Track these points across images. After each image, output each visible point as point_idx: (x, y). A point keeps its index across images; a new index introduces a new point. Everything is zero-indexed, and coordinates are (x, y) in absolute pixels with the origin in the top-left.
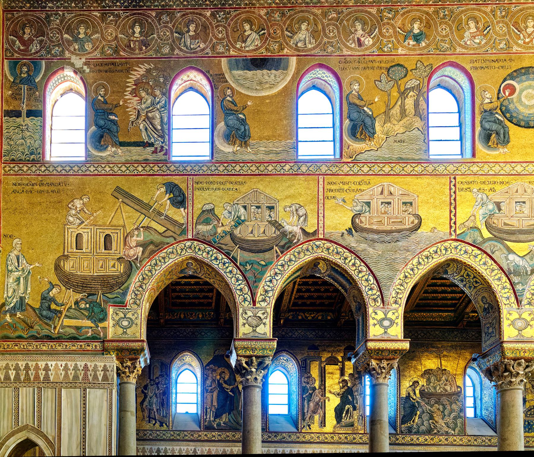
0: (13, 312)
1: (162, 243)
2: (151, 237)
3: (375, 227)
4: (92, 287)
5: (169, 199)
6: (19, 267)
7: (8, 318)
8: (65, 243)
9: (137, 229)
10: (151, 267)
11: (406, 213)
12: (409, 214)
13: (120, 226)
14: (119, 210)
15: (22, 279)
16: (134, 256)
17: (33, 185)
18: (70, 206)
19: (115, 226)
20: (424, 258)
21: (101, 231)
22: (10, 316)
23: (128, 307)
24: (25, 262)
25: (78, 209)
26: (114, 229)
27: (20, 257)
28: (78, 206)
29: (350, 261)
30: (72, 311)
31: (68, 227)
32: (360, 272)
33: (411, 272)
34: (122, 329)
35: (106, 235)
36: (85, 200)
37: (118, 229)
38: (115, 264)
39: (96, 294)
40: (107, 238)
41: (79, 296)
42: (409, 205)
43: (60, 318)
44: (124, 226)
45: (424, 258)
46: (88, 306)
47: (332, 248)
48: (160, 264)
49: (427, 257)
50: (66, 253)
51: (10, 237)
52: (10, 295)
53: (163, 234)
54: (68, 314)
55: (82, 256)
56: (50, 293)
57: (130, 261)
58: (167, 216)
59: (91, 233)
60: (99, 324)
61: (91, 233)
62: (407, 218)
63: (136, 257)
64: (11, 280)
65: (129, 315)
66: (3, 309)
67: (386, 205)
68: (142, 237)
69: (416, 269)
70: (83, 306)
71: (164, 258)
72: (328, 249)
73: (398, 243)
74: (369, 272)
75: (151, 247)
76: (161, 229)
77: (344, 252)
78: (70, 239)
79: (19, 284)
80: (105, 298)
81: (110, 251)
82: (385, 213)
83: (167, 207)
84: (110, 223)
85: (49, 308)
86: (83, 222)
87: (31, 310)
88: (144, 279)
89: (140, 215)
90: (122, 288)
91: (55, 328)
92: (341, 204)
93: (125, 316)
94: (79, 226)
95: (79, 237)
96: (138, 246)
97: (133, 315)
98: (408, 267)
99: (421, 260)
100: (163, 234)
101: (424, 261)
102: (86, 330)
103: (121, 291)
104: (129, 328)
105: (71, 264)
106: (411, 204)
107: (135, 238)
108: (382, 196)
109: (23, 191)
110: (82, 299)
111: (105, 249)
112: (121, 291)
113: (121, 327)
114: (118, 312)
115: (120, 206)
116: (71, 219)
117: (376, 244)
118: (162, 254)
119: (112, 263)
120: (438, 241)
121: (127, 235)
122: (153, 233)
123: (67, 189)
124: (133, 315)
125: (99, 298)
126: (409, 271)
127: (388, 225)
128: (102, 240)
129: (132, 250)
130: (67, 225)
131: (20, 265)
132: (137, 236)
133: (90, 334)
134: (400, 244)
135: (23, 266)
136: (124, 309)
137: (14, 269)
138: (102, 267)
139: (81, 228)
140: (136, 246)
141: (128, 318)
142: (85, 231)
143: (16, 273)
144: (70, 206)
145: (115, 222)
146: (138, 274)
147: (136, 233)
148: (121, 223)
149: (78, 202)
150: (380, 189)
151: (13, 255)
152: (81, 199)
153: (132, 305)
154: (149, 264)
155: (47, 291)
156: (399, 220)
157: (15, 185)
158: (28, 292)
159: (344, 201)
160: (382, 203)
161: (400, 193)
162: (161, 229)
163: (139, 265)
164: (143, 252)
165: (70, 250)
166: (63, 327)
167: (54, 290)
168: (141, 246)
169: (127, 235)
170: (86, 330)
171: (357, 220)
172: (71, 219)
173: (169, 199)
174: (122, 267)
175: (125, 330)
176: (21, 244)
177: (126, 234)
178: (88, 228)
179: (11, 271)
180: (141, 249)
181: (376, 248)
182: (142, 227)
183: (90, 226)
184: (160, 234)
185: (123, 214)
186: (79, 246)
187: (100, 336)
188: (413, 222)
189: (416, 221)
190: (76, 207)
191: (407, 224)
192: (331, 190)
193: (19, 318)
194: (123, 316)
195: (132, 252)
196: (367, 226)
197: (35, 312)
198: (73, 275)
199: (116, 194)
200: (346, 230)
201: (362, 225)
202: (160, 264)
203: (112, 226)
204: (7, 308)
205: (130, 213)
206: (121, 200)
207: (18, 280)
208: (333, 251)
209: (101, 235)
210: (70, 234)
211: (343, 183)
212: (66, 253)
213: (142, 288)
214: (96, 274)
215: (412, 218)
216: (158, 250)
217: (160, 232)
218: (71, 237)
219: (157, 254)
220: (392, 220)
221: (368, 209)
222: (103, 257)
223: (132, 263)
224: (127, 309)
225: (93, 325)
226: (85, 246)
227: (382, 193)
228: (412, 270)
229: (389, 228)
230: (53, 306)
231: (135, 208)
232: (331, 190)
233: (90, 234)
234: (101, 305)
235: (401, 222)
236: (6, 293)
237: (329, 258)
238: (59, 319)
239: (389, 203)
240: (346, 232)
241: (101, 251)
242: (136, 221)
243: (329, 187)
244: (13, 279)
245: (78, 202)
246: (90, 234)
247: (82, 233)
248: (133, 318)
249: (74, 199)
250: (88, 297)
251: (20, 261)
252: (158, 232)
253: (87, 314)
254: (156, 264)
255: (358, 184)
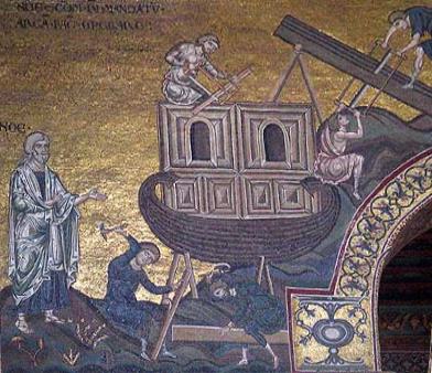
0: (33, 312)
1: (414, 145)
2: (385, 131)
4: (241, 249)
5: (421, 44)
6: (44, 199)
7: (21, 324)
8: (162, 144)
9: (346, 112)
10: (387, 201)
13: (302, 107)
14: (297, 71)
15: (54, 230)
16: (343, 173)
17: (71, 9)
18: (170, 58)
19: (290, 105)
21: (252, 116)
22: (27, 320)
23: (335, 295)
24: (59, 189)
25: (192, 66)
26: (287, 113)
27: (47, 178)
28: (192, 59)
30: (192, 304)
31: (168, 106)
34: (325, 349)
35: (268, 126)
36: (207, 45)
37: (298, 113)
38: (296, 193)
39: (252, 265)
40: (272, 134)
41: (209, 269)
43: (162, 322)
44: (312, 106)
46: (233, 292)
48: (410, 193)
50: (167, 169)
51: (17, 128)
52: (23, 266)
53: (414, 125)
54: (183, 312)
55: (209, 176)
56: (133, 262)
57: (333, 187)
58: (418, 83)
59: (229, 117)
60: (266, 337)
61: (229, 117)
63: (348, 177)
64: (25, 232)
65: (341, 314)
66: (9, 301)
68: (360, 132)
70: (221, 293)
71: (418, 179)
75: (386, 152)
76: (407, 113)
78: (175, 135)
79: (46, 242)
80: (277, 274)
81: (283, 164)
83: (419, 63)
84: (276, 97)
85: (130, 298)
86: (205, 97)
87: (83, 305)
88: (371, 227)
89: (351, 82)
90: (318, 249)
91: (150, 348)
93: (331, 316)
94: (196, 106)
95: (198, 131)
96: (352, 152)
97: (352, 313)
100: (414, 125)
102: (235, 350)
103: (319, 258)
104: (343, 345)
105: (183, 193)
107: (341, 133)
109: (46, 23)
110: (216, 277)
111: (268, 159)
112: (319, 258)
113: (324, 344)
114: (310, 307)
115: (297, 58)
116: (174, 88)
118: (415, 171)
119: (287, 190)
121: (323, 126)
122: (387, 122)
123: (161, 20)
124: (352, 313)
125: (263, 271)
128: (259, 137)
129: (337, 160)
130: (167, 102)
131: (48, 195)
132: (348, 128)
133: (244, 360)
135: (57, 198)
136: (326, 299)
137: (32, 206)
138: (262, 200)
139: (203, 110)
140: (345, 153)
141: (336, 321)
142: (214, 116)
143: (38, 216)
144: (170, 58)
145: (287, 97)
146: (356, 218)
147: (344, 120)
148: (305, 98)
149: (191, 50)
151: (28, 172)
152: (197, 43)
153: (348, 291)
154: (382, 193)
155: (125, 259)
157: (25, 9)
158: (73, 260)
162: (407, 113)
163: (357, 196)
164: (365, 167)
165: (176, 161)
166: (173, 345)
167: (142, 256)
168: (358, 151)
169: (323, 126)
170: (235, 350)
172: (175, 89)
173: (421, 44)
174: (315, 200)
175: (334, 351)
176: (47, 146)
177: (318, 125)
178: (220, 111)
179: (24, 210)
180: (360, 159)
182: (358, 108)
183: (225, 104)
184: (407, 124)
185: (308, 77)
186: (200, 148)
187: (272, 364)
190: (187, 61)
193: (53, 323)
194: (325, 316)
195: (337, 166)
197: (95, 309)
198: (187, 218)
199: (286, 33)
202: (410, 193)
203: (281, 106)
204: (18, 299)
205: (326, 75)
206: (299, 47)
207: (43, 232)
209: (256, 124)
210: (174, 124)
212: (167, 169)
213: (370, 250)
214: (247, 217)
216: (404, 160)
217: (404, 118)
218: (179, 130)
219: (401, 170)
222: (263, 177)
223: (341, 192)
224: (334, 299)
225: (251, 339)
226: (215, 150)
230: (142, 294)
231: (336, 62)
233: (225, 123)
234: (268, 291)
236: (13, 262)
238: (162, 326)
241: (258, 163)
242: (343, 95)
244: (31, 230)
245: (191, 50)
246: (225, 123)
247: (207, 121)
248: (353, 322)
249: (181, 43)
250: (233, 269)
251: (48, 186)
252: (403, 121)
253: (232, 313)
254: (400, 194)
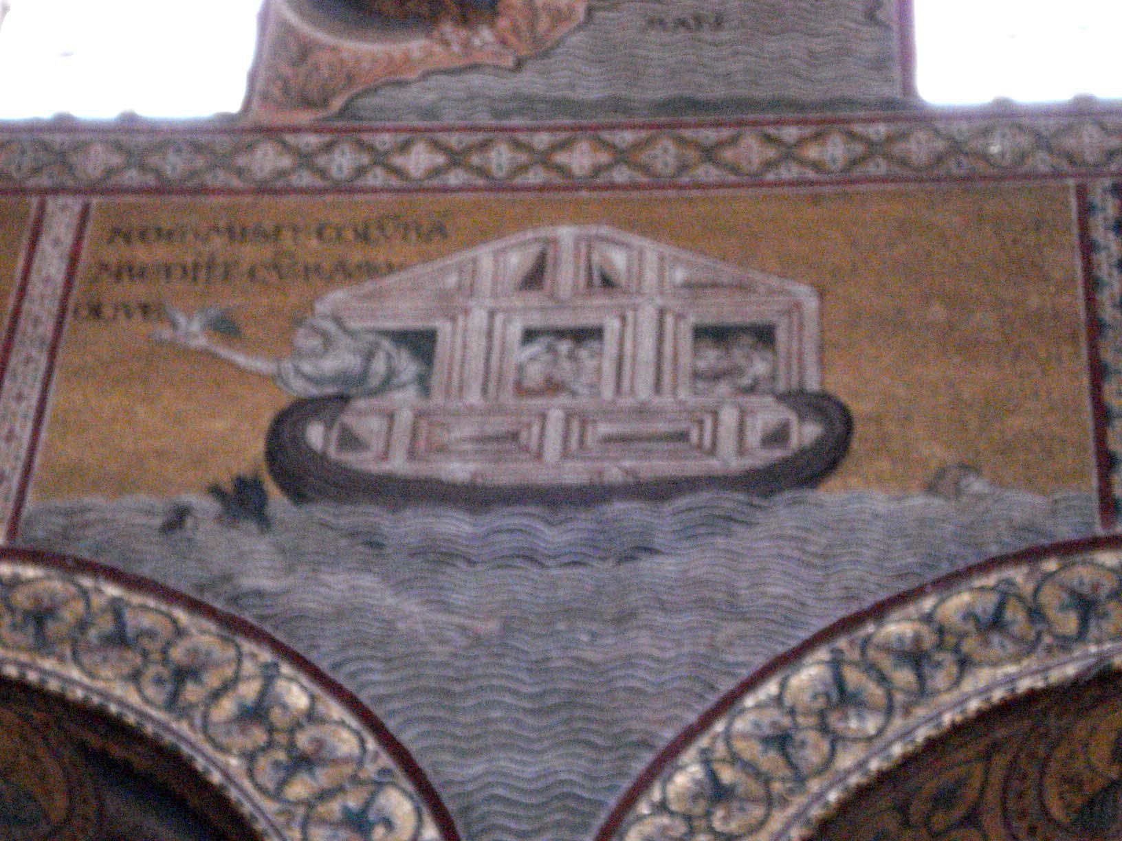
3: (457, 470)
11: (723, 388)
12: (751, 390)
20: (886, 663)
29: (216, 695)
32: (302, 762)
33: (769, 760)
42: (747, 340)
45: (886, 663)
47: (71, 613)
49: (915, 657)
62: (729, 417)
67: (564, 347)
69: (812, 736)
72: (40, 616)
73: (646, 564)
74: (386, 760)
77: (180, 632)
82: (553, 387)
92: (201, 342)
98: (741, 725)
99: (853, 677)
101: (882, 679)
106: (764, 336)
108: (533, 298)
117: (457, 574)
120: (994, 550)
126: (749, 750)
127: (566, 454)
134: (665, 567)
150: (518, 261)
156: (662, 427)
159: (226, 328)
160: (529, 335)
161: (680, 275)
171: (315, 434)
181: (458, 599)
188: (777, 436)
189: (807, 433)
191: (728, 444)
192: (126, 271)
196: (398, 464)
200: (216, 491)
201: (352, 459)
208: (83, 625)
211: (235, 234)
215: (768, 414)
220: (604, 429)
221: (408, 367)
227: (535, 278)
228: (781, 741)
229: (574, 474)
232: (126, 271)
235: (683, 436)
237: (32, 677)
239: (585, 335)
240: (206, 506)
243: (114, 254)
255: (349, 235)
